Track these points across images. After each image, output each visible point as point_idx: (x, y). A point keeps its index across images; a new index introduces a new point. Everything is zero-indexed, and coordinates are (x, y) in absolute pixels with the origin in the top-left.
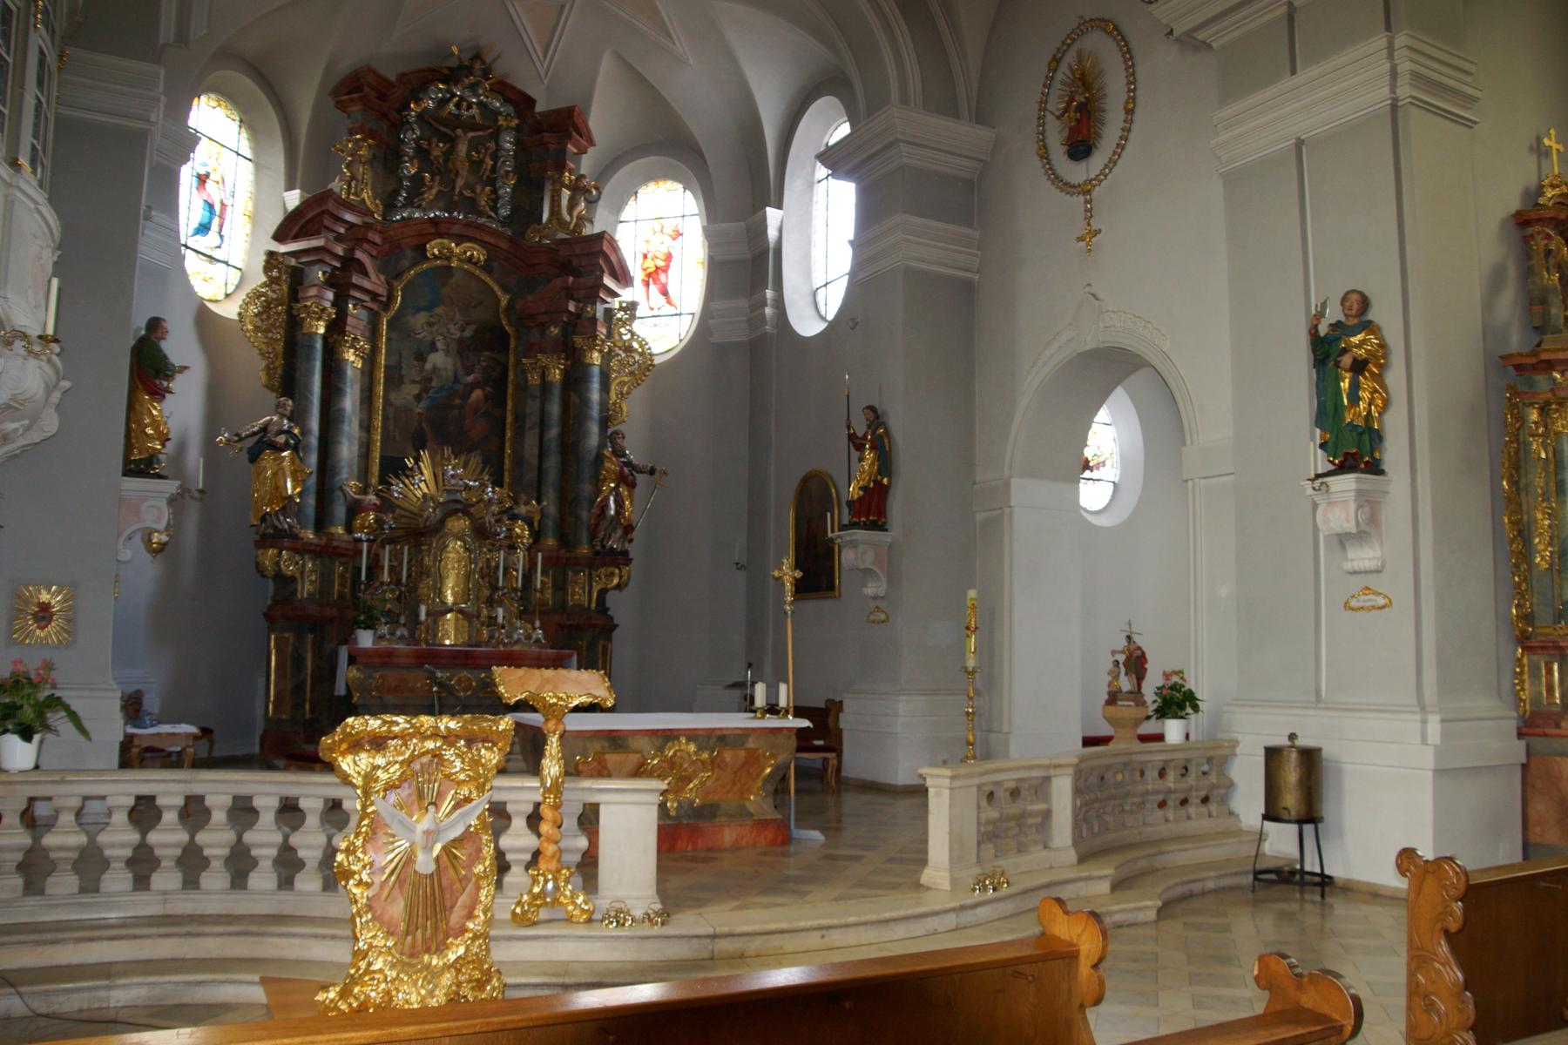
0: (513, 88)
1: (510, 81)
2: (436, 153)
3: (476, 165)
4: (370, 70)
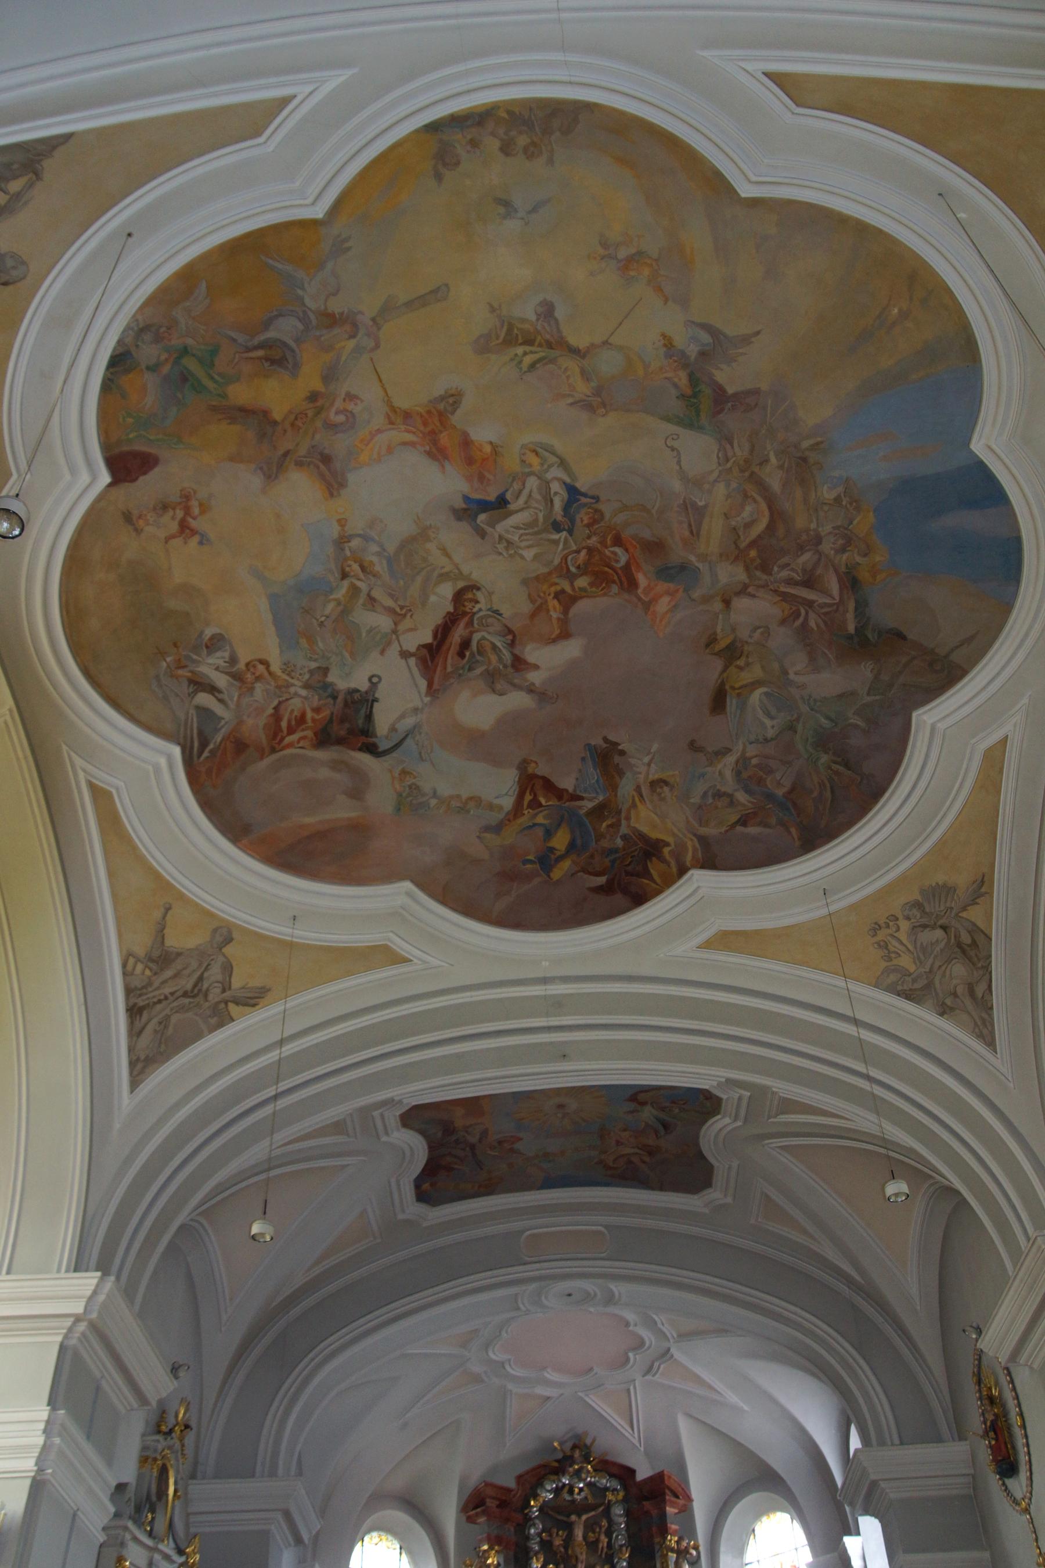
0: (614, 1464)
1: (608, 1458)
2: (558, 1542)
3: (592, 1546)
4: (487, 1484)
